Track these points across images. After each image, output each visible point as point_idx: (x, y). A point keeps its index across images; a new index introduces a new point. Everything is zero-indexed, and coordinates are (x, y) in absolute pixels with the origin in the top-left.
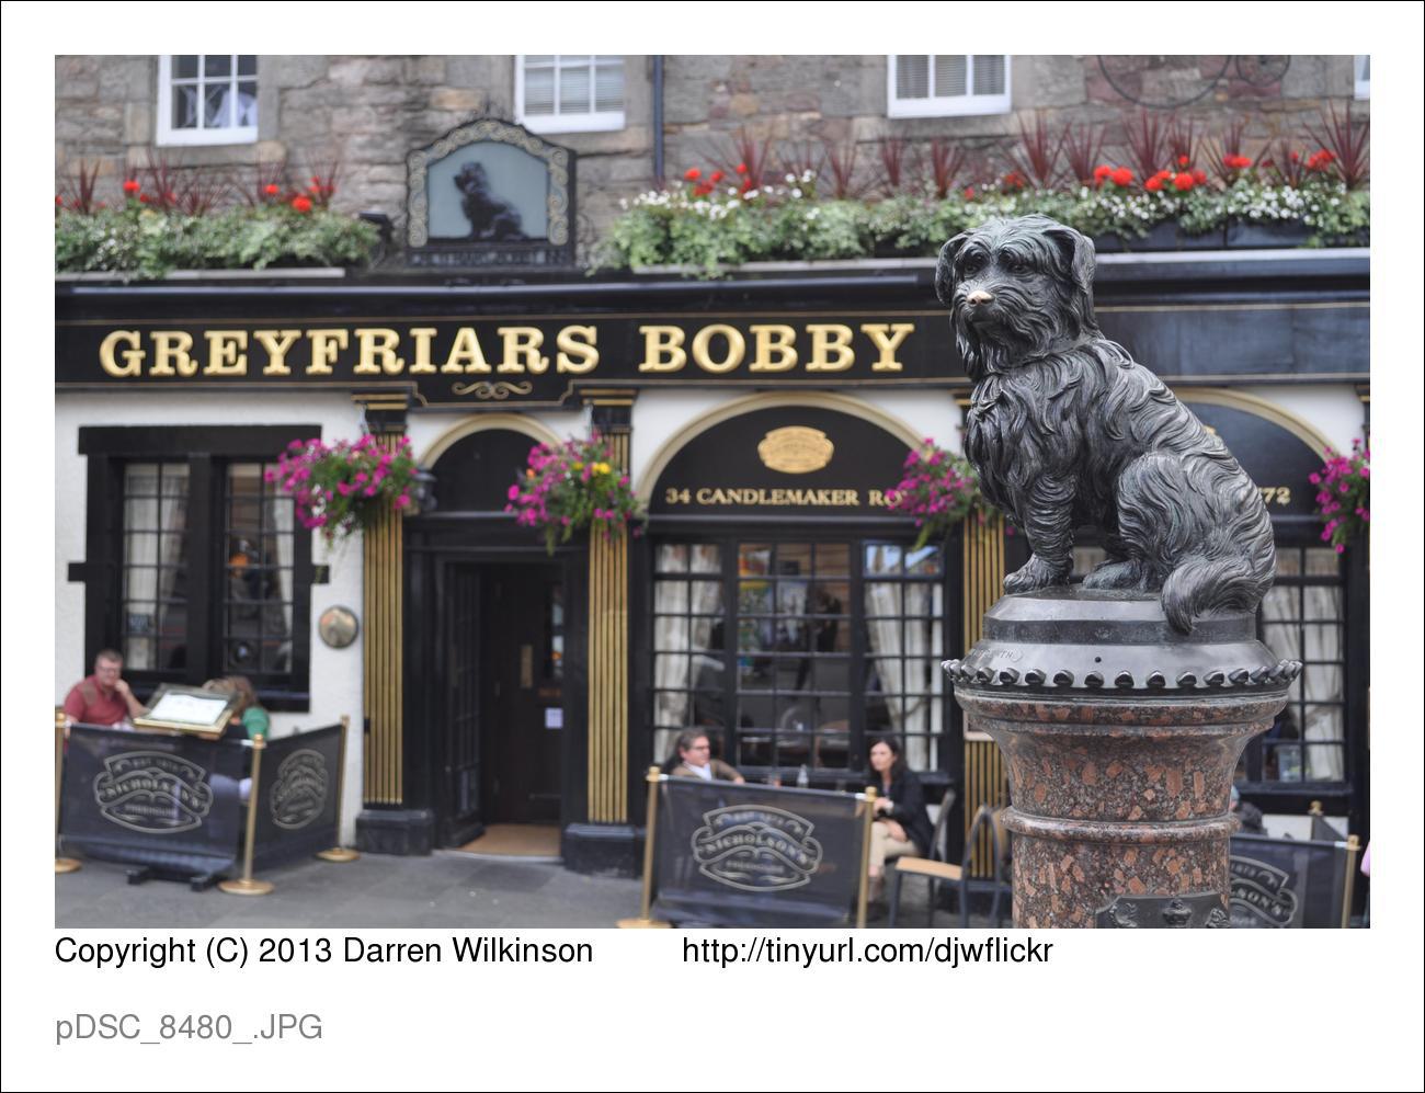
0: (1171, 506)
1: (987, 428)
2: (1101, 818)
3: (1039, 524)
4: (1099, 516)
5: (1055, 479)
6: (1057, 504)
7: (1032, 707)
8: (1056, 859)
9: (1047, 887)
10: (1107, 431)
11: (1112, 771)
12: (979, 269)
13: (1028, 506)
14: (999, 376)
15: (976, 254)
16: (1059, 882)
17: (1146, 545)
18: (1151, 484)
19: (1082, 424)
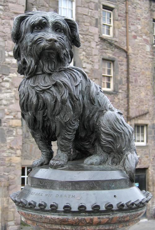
0: (122, 131)
1: (47, 96)
3: (67, 138)
4: (82, 136)
5: (75, 120)
6: (74, 129)
7: (92, 220)
10: (92, 101)
12: (42, 28)
13: (64, 131)
14: (50, 75)
15: (45, 22)
17: (113, 147)
18: (115, 122)
19: (83, 97)
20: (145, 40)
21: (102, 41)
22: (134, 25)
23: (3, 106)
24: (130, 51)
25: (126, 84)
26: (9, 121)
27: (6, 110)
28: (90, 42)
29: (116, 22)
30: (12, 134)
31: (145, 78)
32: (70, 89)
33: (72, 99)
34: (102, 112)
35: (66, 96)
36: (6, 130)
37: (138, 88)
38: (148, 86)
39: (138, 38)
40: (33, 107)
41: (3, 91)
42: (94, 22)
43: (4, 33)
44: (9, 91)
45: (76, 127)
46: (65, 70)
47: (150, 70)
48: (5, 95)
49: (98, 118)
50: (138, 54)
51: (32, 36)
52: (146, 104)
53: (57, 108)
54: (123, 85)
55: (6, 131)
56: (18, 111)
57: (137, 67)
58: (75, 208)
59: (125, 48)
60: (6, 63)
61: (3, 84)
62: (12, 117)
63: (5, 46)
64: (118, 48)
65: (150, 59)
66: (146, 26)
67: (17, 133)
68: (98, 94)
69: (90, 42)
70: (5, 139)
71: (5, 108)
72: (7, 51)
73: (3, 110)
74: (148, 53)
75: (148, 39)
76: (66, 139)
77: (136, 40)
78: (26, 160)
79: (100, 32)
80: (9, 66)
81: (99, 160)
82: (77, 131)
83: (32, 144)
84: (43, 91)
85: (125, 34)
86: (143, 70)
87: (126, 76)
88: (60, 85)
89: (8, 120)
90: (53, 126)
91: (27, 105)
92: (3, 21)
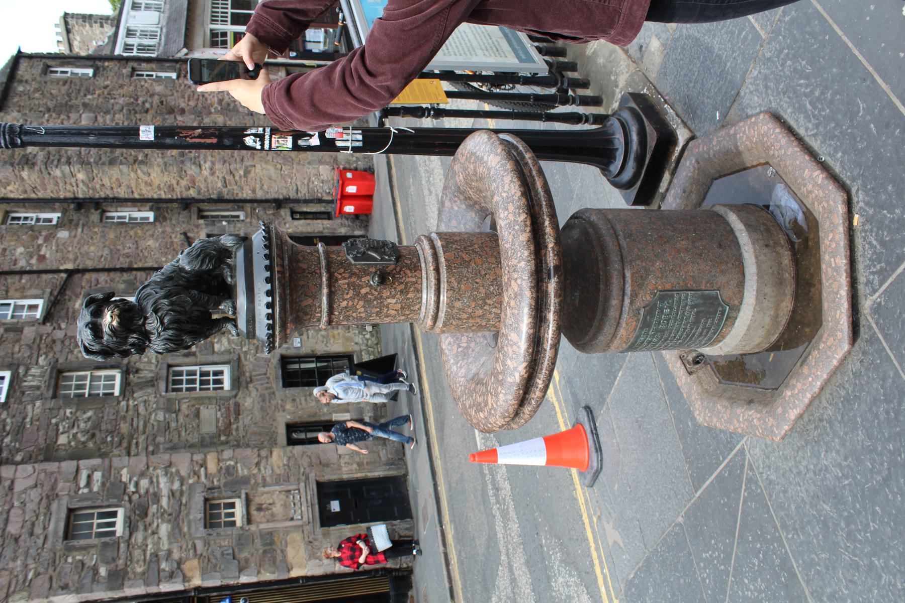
2: (319, 263)
8: (337, 280)
9: (348, 284)
11: (301, 259)
12: (98, 328)
16: (345, 279)
20: (47, 239)
21: (51, 319)
22: (16, 260)
23: (184, 488)
24: (70, 266)
25: (134, 273)
26: (211, 474)
27: (191, 481)
28: (54, 341)
29: (10, 294)
30: (234, 468)
31: (122, 239)
32: (159, 299)
33: (170, 295)
34: (182, 270)
35: (166, 301)
36: (226, 478)
37: (142, 251)
38: (136, 233)
39: (42, 253)
40: (177, 333)
41: (156, 489)
42: (11, 335)
43: (41, 500)
44: (155, 480)
45: (196, 292)
46: (140, 305)
47: (106, 230)
48: (162, 486)
49: (187, 272)
50: (76, 253)
51: (105, 338)
52: (171, 237)
53: (178, 308)
54: (136, 278)
55: (229, 478)
56: (192, 460)
57: (100, 254)
58: (269, 287)
59: (64, 275)
60: (103, 491)
61: (142, 491)
62: (203, 469)
63: (68, 494)
64: (65, 290)
65: (85, 232)
66: (19, 237)
67: (230, 459)
68: (163, 274)
69: (54, 341)
70: (242, 478)
71: (187, 483)
72: (79, 490)
73: (191, 485)
74: (73, 234)
75: (44, 233)
76: (208, 301)
77: (48, 256)
78: (278, 442)
79: (33, 322)
80: (108, 485)
81: (228, 270)
82: (201, 291)
83: (249, 434)
84: (162, 323)
85: (35, 276)
86: (107, 243)
87: (118, 274)
88: (155, 308)
89: (208, 476)
90: (196, 313)
91: (176, 340)
92: (16, 504)
